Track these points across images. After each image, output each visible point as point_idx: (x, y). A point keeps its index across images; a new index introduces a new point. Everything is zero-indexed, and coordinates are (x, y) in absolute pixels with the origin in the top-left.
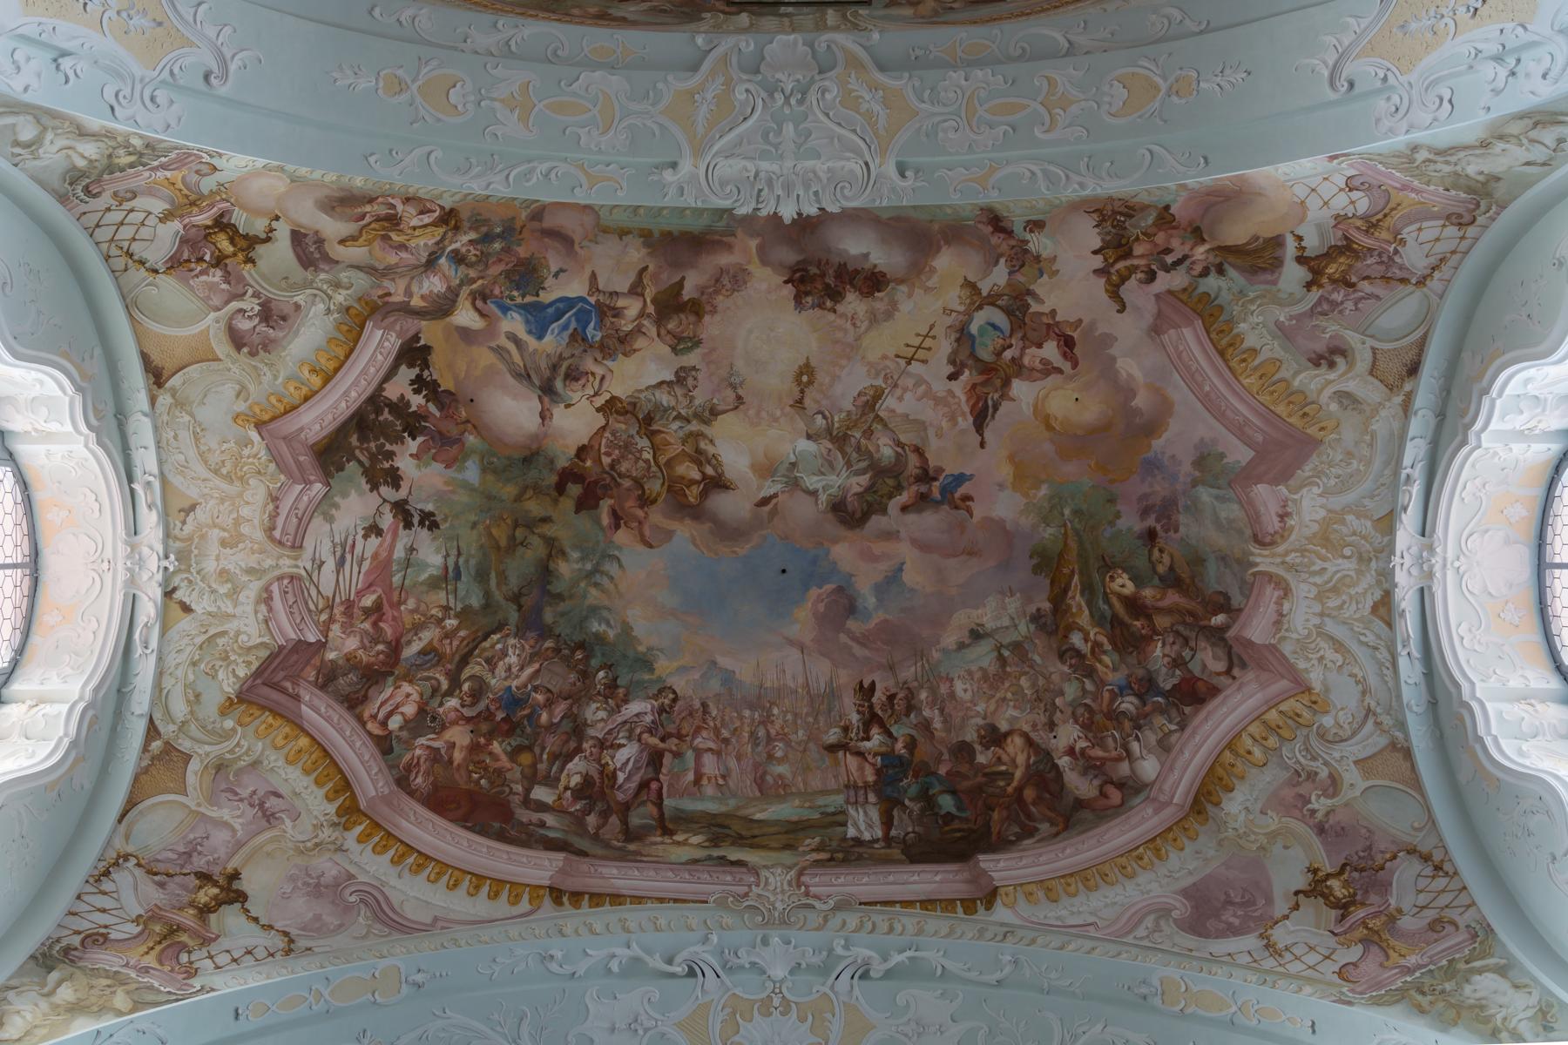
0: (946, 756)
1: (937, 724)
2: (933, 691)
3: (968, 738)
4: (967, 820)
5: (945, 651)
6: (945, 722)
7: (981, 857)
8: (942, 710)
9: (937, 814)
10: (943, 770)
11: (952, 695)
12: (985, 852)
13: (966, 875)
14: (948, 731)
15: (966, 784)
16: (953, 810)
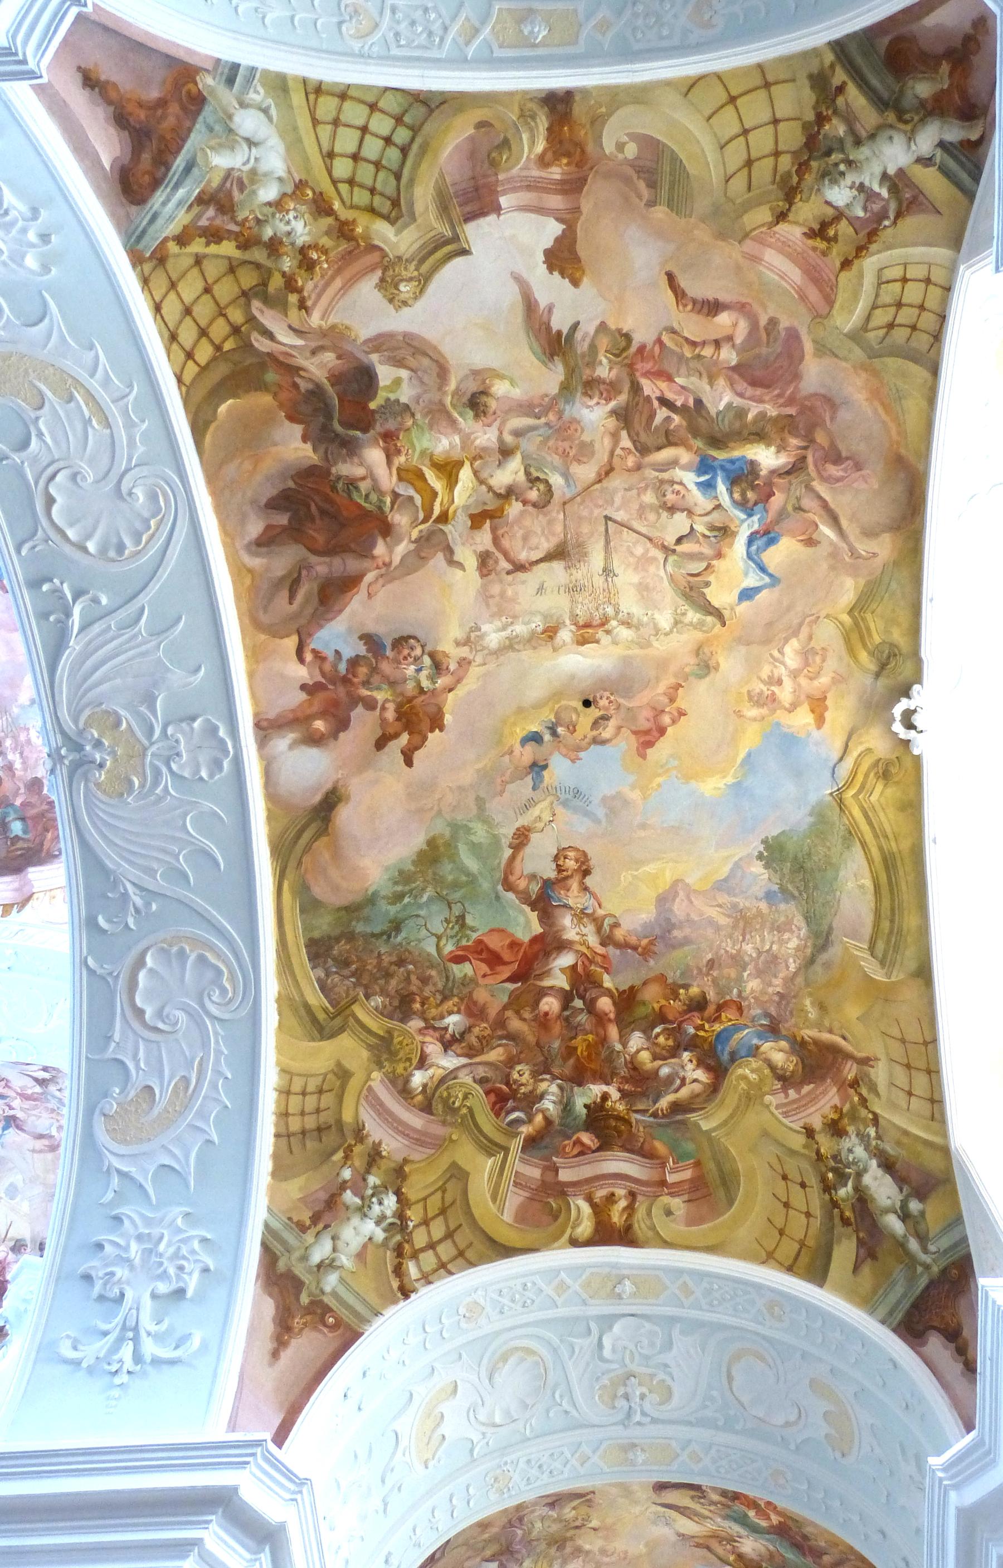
0: (22, 791)
1: (18, 765)
2: (15, 738)
3: (39, 775)
4: (28, 840)
5: (22, 707)
6: (24, 763)
7: (31, 869)
8: (21, 753)
9: (7, 838)
10: (18, 802)
11: (29, 742)
12: (35, 865)
13: (16, 885)
14: (25, 770)
15: (33, 812)
16: (20, 833)
